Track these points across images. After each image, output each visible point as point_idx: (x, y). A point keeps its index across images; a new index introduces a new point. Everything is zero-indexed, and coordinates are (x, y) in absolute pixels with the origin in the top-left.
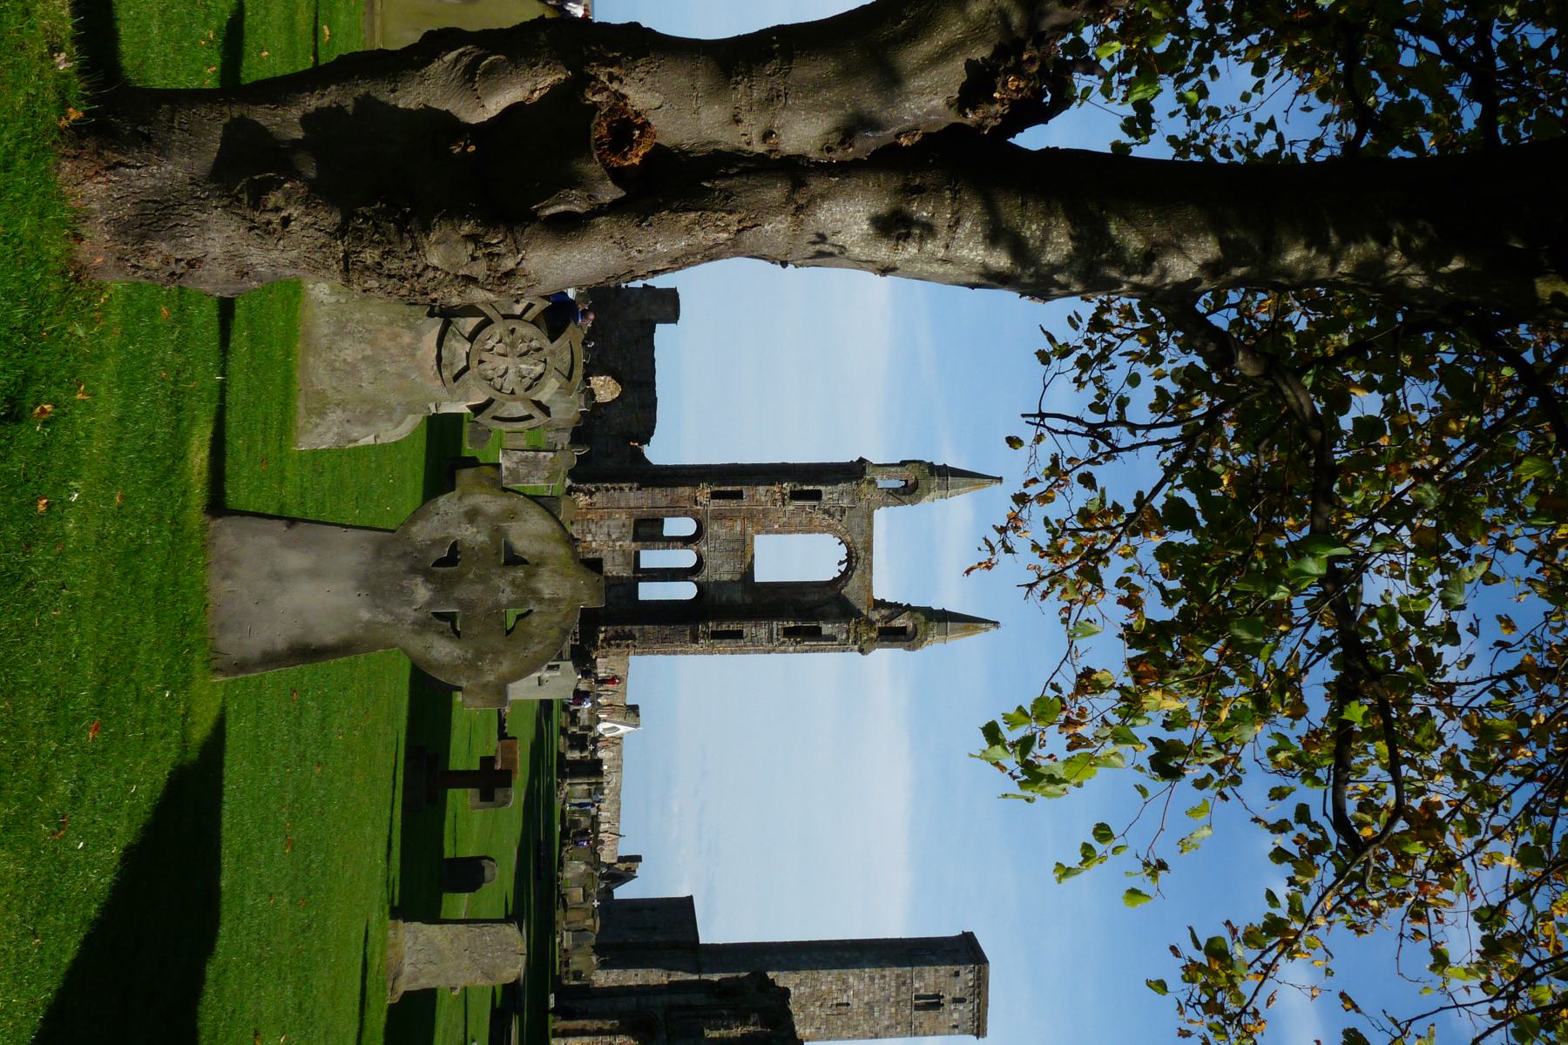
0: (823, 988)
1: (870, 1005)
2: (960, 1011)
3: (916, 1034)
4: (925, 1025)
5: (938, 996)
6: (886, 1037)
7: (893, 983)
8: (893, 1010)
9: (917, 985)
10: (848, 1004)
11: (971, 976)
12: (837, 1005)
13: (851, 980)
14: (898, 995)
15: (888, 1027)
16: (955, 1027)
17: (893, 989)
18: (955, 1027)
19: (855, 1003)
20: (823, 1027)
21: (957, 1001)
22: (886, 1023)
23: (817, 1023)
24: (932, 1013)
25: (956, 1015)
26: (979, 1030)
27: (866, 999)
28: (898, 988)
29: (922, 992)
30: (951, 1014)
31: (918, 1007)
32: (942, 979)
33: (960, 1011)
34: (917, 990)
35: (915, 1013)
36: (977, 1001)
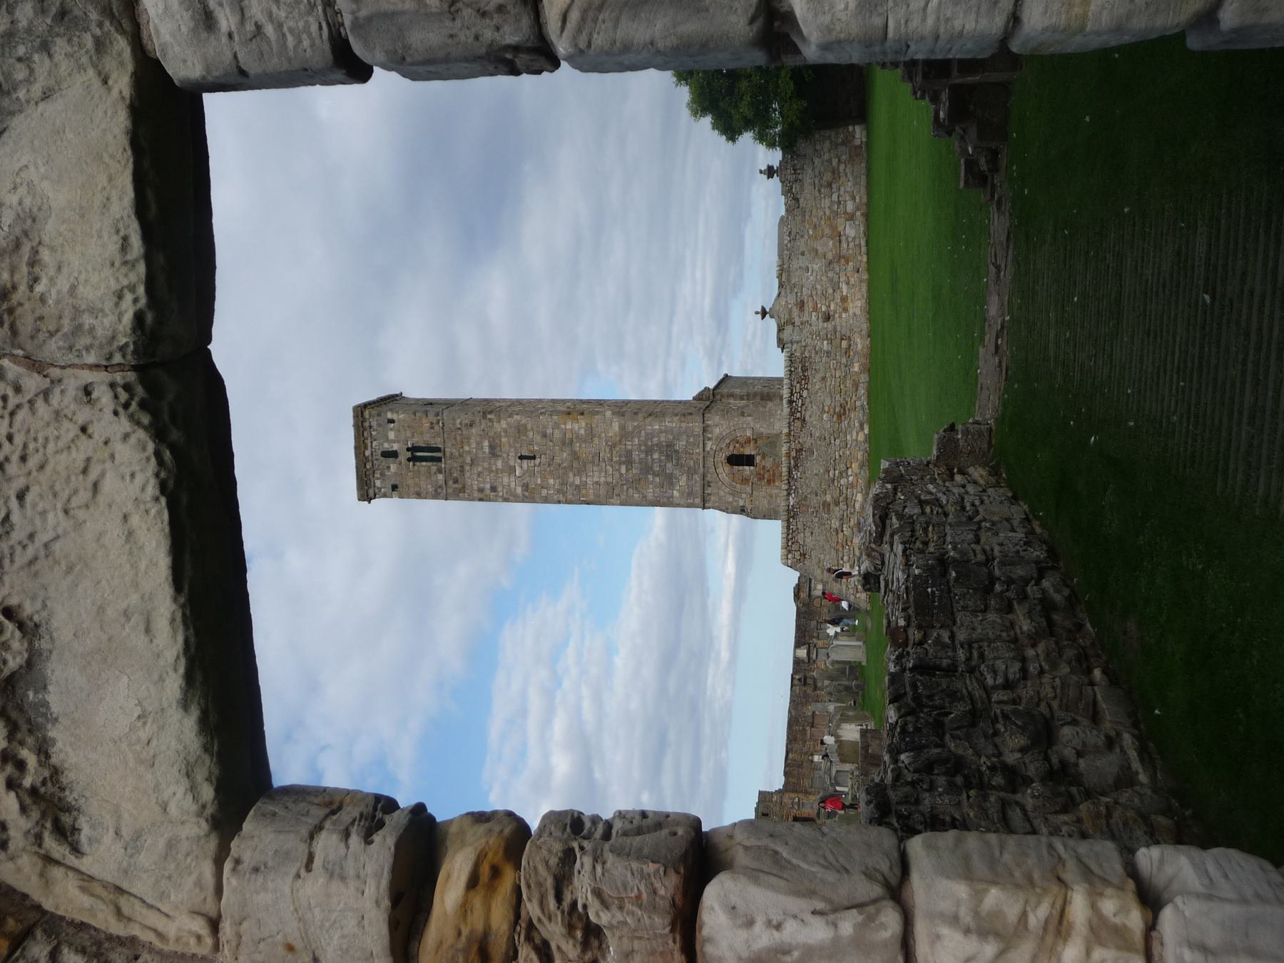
0: (551, 481)
2: (387, 440)
5: (414, 459)
9: (440, 477)
10: (521, 458)
11: (378, 483)
12: (534, 458)
14: (462, 467)
15: (471, 425)
18: (392, 421)
19: (513, 461)
21: (394, 454)
27: (499, 464)
31: (438, 450)
32: (410, 482)
33: (387, 440)
34: (440, 471)
35: (438, 442)
36: (368, 453)
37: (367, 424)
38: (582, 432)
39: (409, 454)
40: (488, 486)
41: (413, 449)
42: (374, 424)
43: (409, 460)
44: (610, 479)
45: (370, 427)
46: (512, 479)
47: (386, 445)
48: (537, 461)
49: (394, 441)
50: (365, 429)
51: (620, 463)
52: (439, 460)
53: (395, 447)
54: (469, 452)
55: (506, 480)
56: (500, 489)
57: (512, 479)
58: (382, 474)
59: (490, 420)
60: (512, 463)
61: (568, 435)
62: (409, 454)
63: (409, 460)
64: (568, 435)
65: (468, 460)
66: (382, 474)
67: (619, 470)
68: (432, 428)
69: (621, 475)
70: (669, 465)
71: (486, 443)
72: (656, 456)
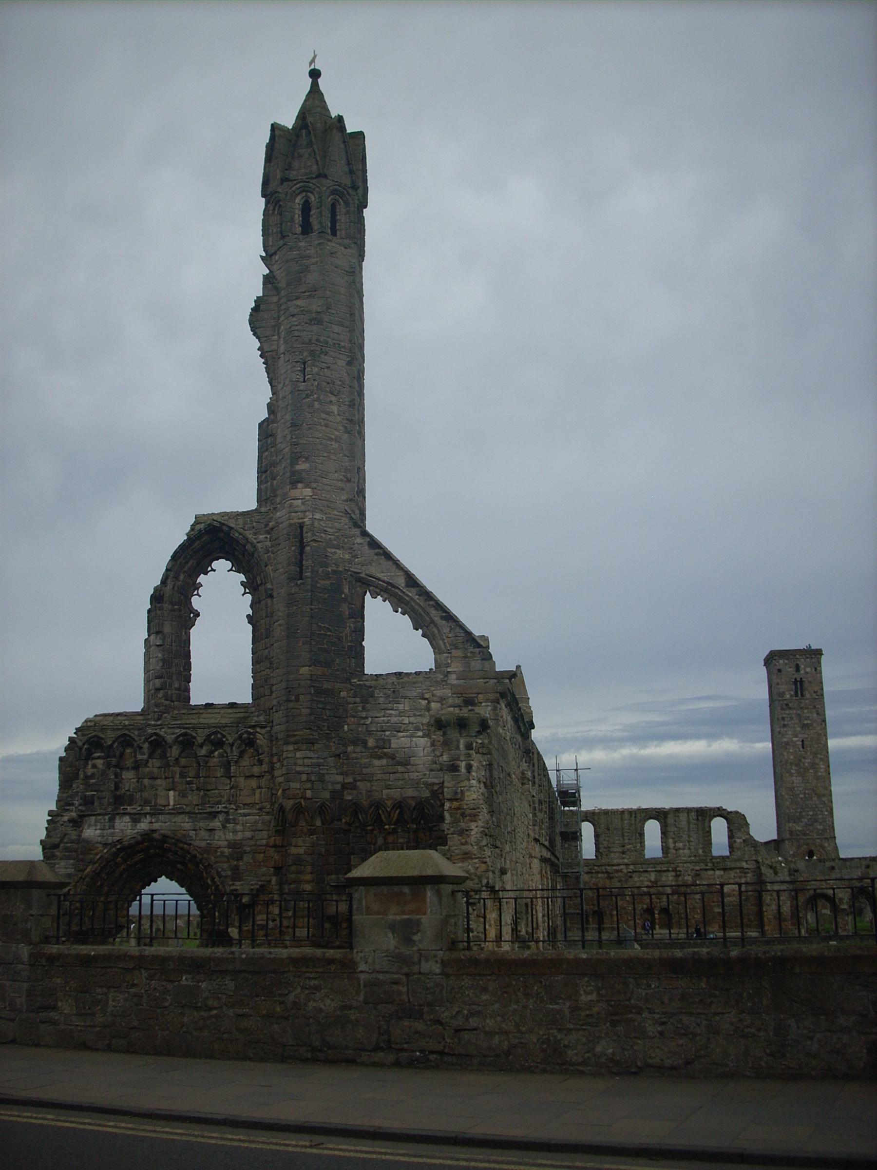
1: (804, 726)
2: (806, 667)
3: (822, 695)
4: (816, 690)
6: (825, 715)
7: (787, 712)
8: (806, 711)
9: (788, 696)
10: (803, 741)
11: (781, 661)
12: (803, 748)
13: (785, 740)
14: (795, 708)
15: (818, 714)
16: (816, 669)
17: (791, 712)
18: (816, 669)
20: (819, 756)
22: (815, 715)
23: (817, 761)
24: (806, 685)
25: (808, 670)
26: (819, 653)
27: (798, 729)
28: (790, 708)
29: (792, 693)
30: (807, 673)
31: (802, 695)
34: (791, 696)
35: (808, 696)
37: (813, 656)
38: (820, 774)
39: (798, 679)
40: (786, 723)
41: (801, 681)
42: (813, 660)
43: (796, 679)
44: (796, 789)
45: (812, 658)
46: (791, 736)
47: (802, 666)
48: (801, 749)
49: (805, 670)
50: (810, 655)
51: (805, 794)
52: (797, 696)
53: (802, 672)
54: (804, 713)
55: (790, 732)
56: (785, 729)
57: (791, 736)
58: (786, 664)
59: (821, 724)
60: (800, 736)
61: (817, 766)
62: (798, 679)
63: (796, 679)
64: (817, 766)
65: (799, 712)
66: (786, 664)
67: (801, 793)
68: (814, 692)
69: (799, 795)
70: (806, 820)
71: (809, 722)
72: (811, 813)
